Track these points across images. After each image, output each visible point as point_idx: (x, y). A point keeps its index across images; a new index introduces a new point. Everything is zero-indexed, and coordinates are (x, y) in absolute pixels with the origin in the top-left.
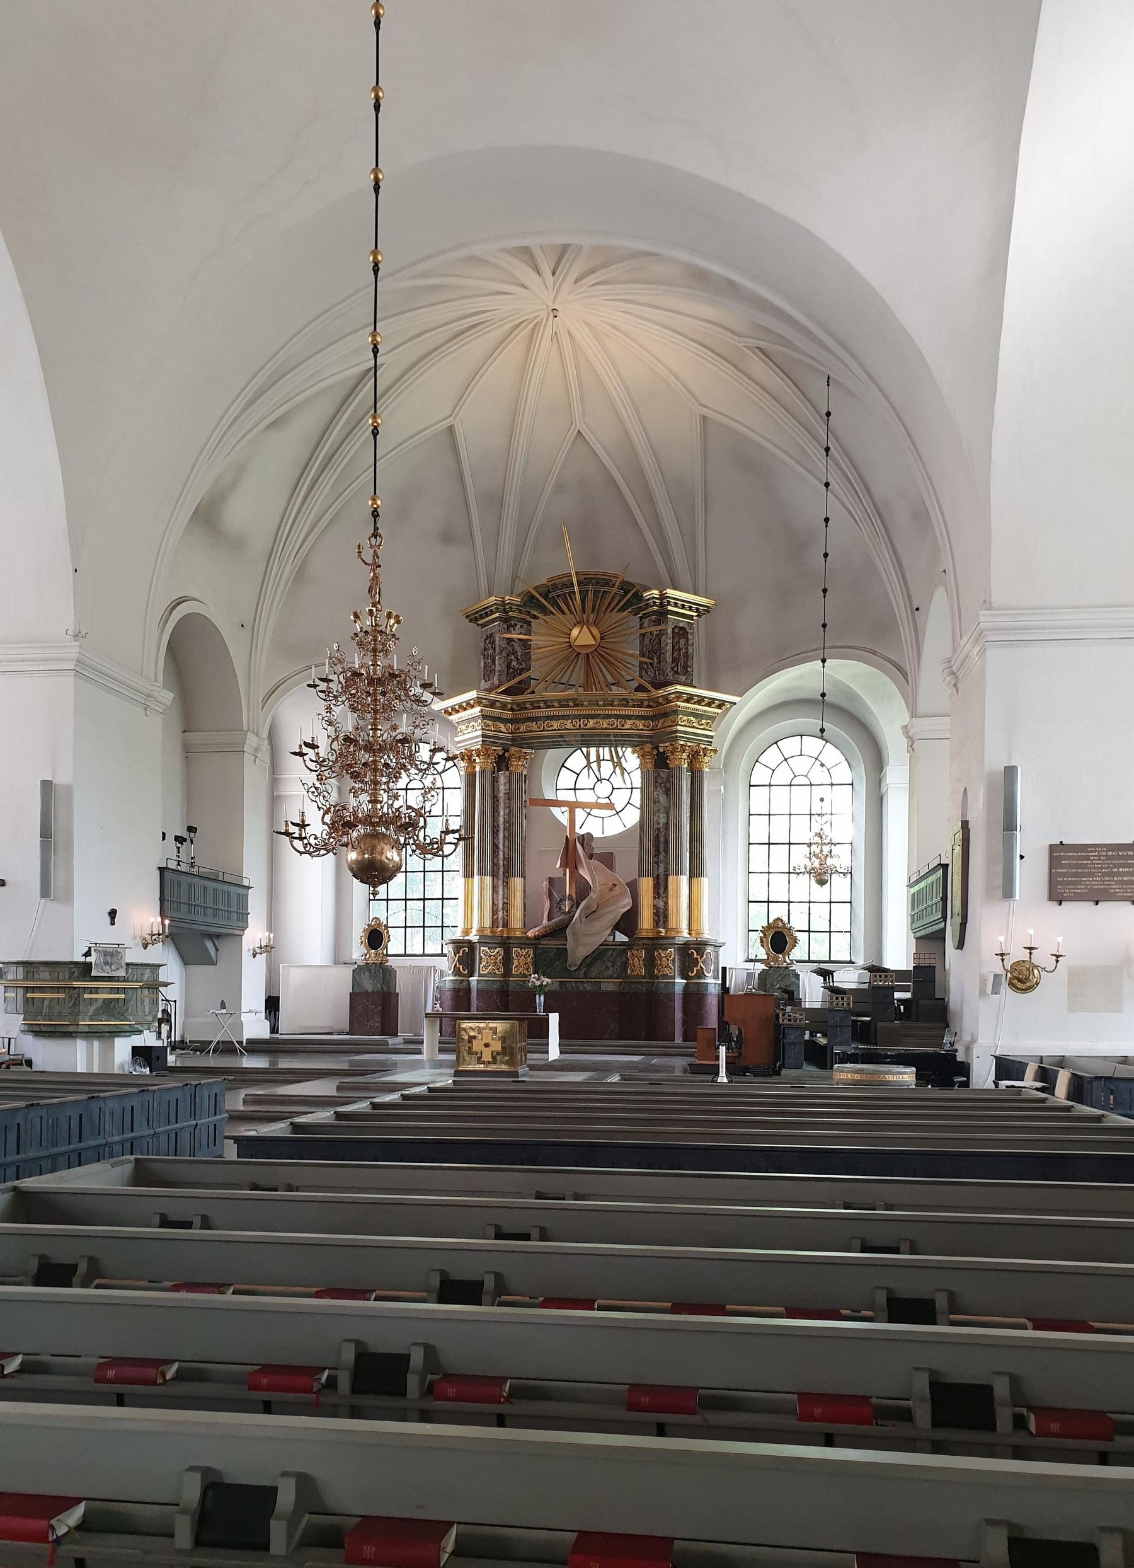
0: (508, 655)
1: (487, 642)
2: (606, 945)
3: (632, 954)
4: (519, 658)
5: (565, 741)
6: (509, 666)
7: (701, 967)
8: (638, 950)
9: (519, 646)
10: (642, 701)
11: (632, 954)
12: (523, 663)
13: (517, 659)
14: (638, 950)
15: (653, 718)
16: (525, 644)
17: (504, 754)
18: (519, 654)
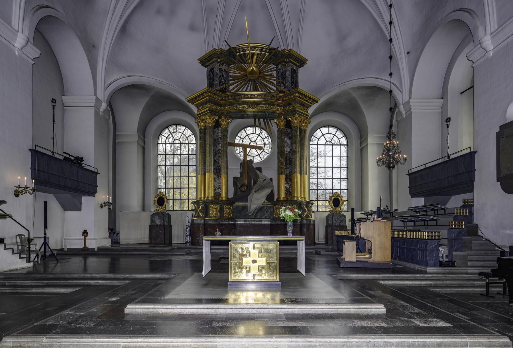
0: (220, 77)
1: (210, 72)
2: (265, 204)
3: (276, 208)
4: (225, 78)
5: (246, 114)
6: (220, 82)
7: (307, 213)
8: (279, 206)
9: (225, 73)
10: (280, 97)
11: (276, 208)
12: (226, 81)
13: (224, 79)
14: (279, 206)
15: (284, 106)
16: (227, 73)
17: (219, 119)
18: (225, 77)
